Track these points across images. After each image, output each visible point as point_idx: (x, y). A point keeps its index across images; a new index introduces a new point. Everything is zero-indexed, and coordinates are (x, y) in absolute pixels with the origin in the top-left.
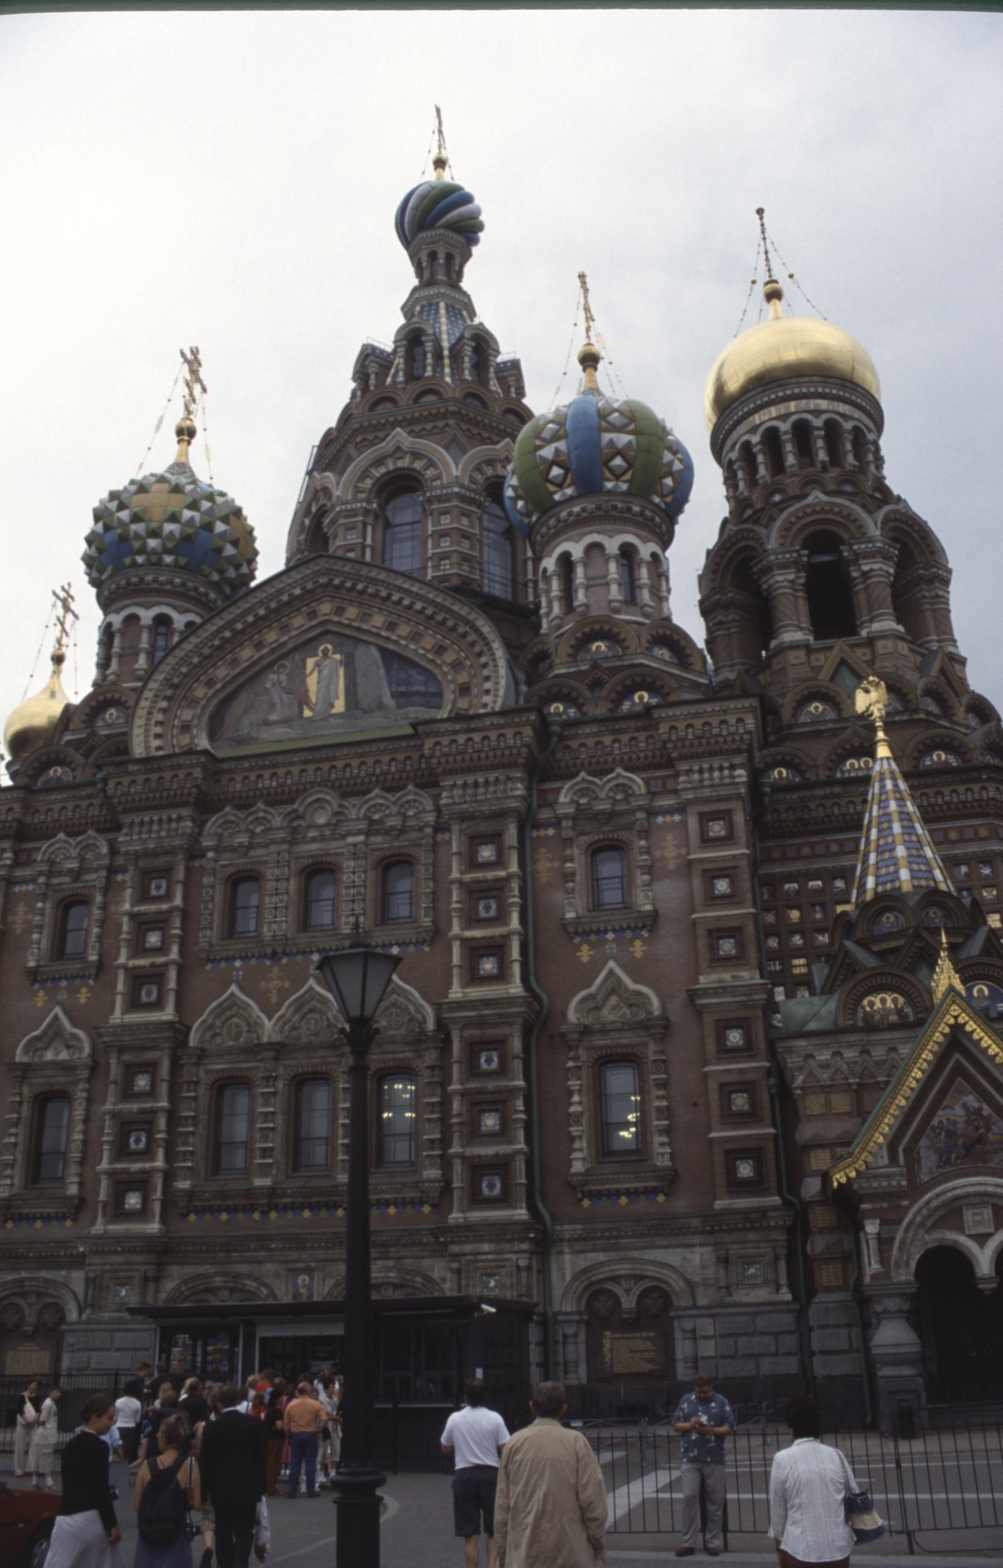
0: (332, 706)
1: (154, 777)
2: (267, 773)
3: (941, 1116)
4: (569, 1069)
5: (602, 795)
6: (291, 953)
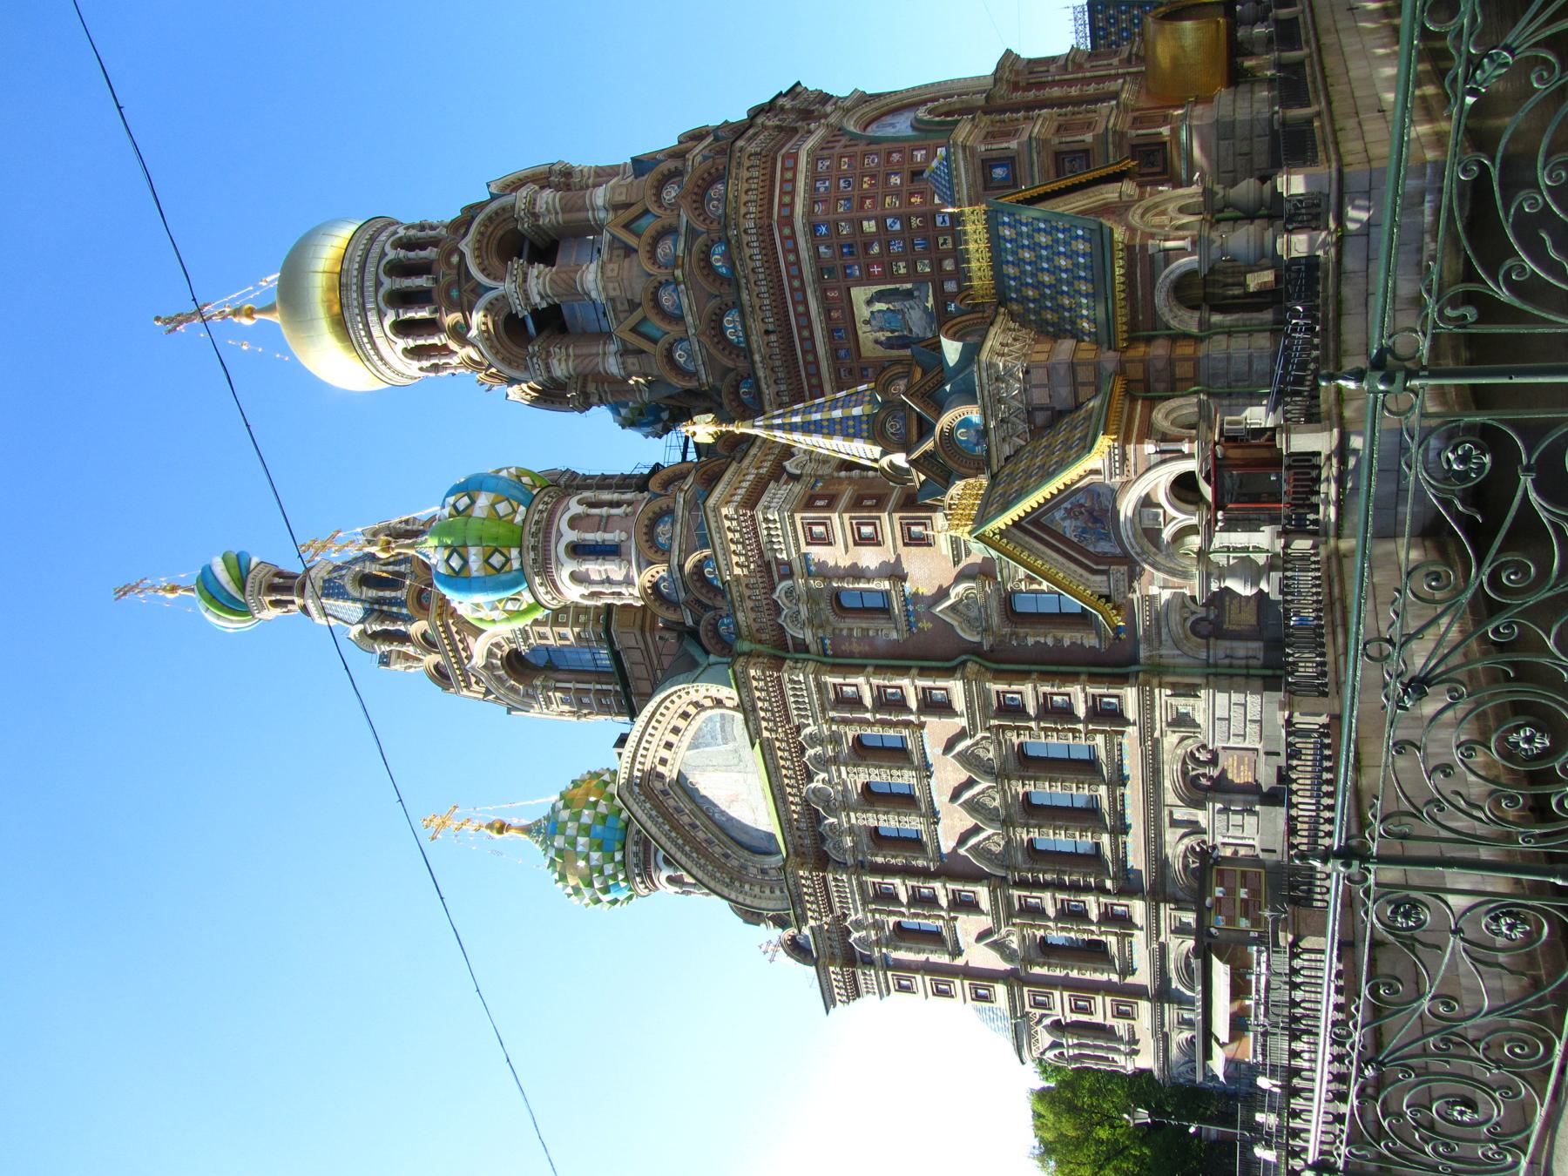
3: (1070, 535)
4: (1019, 645)
5: (795, 608)
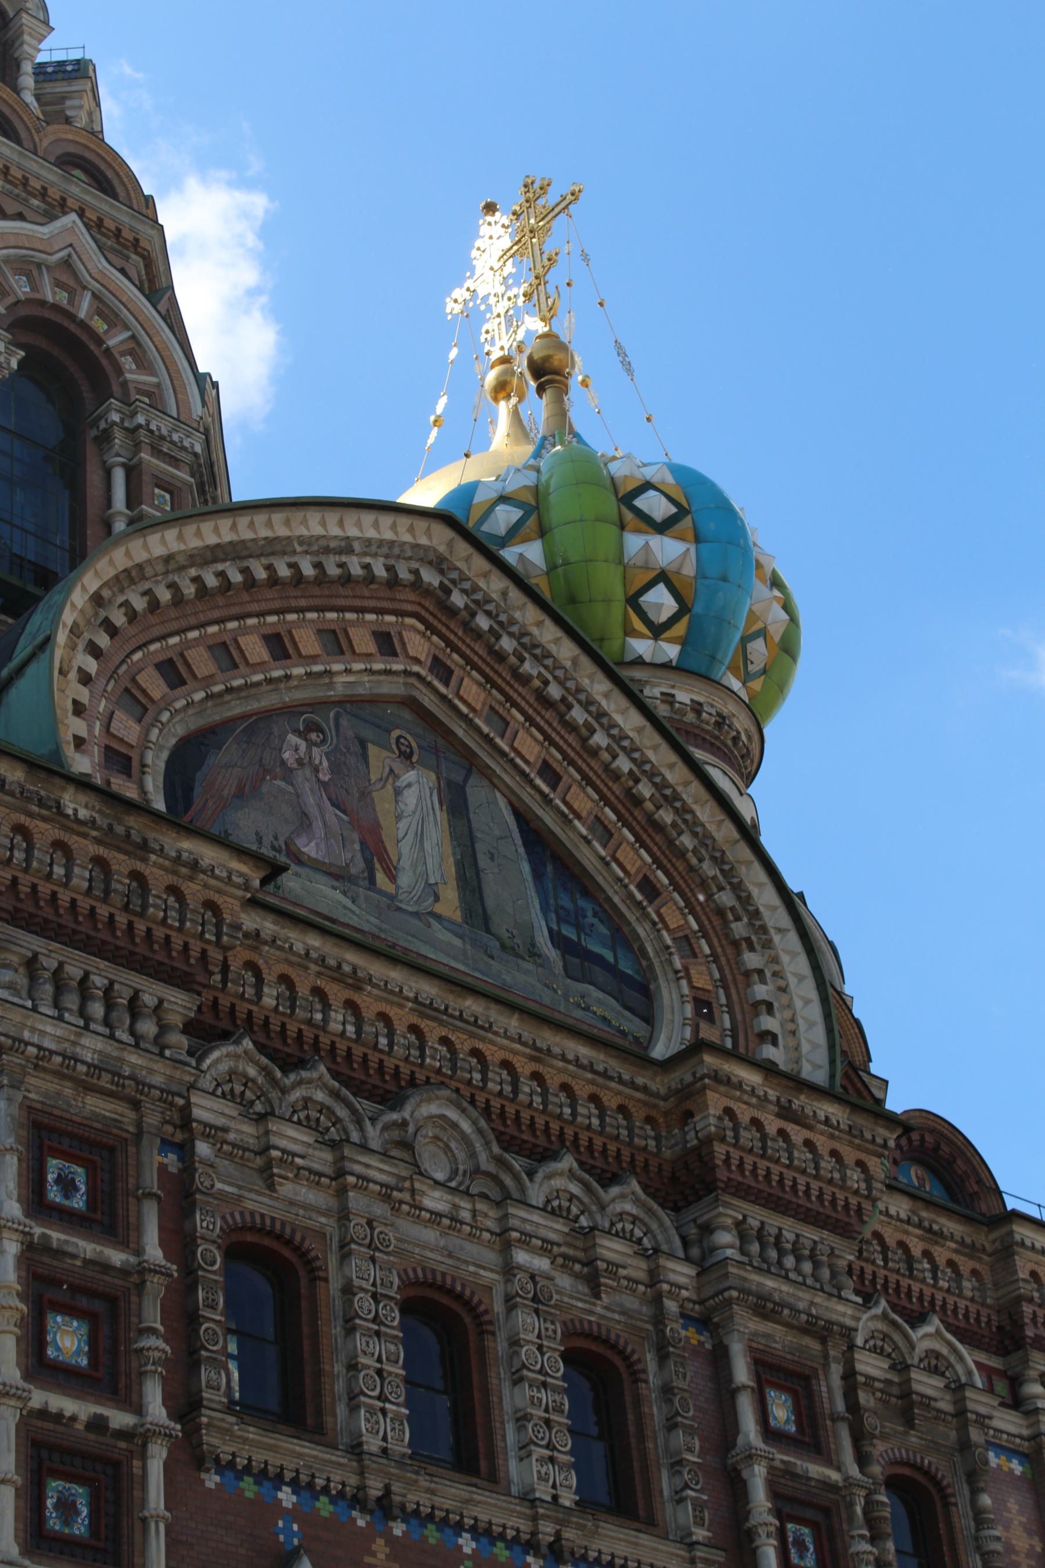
0: (437, 899)
1: (121, 863)
2: (337, 993)
6: (416, 1513)
